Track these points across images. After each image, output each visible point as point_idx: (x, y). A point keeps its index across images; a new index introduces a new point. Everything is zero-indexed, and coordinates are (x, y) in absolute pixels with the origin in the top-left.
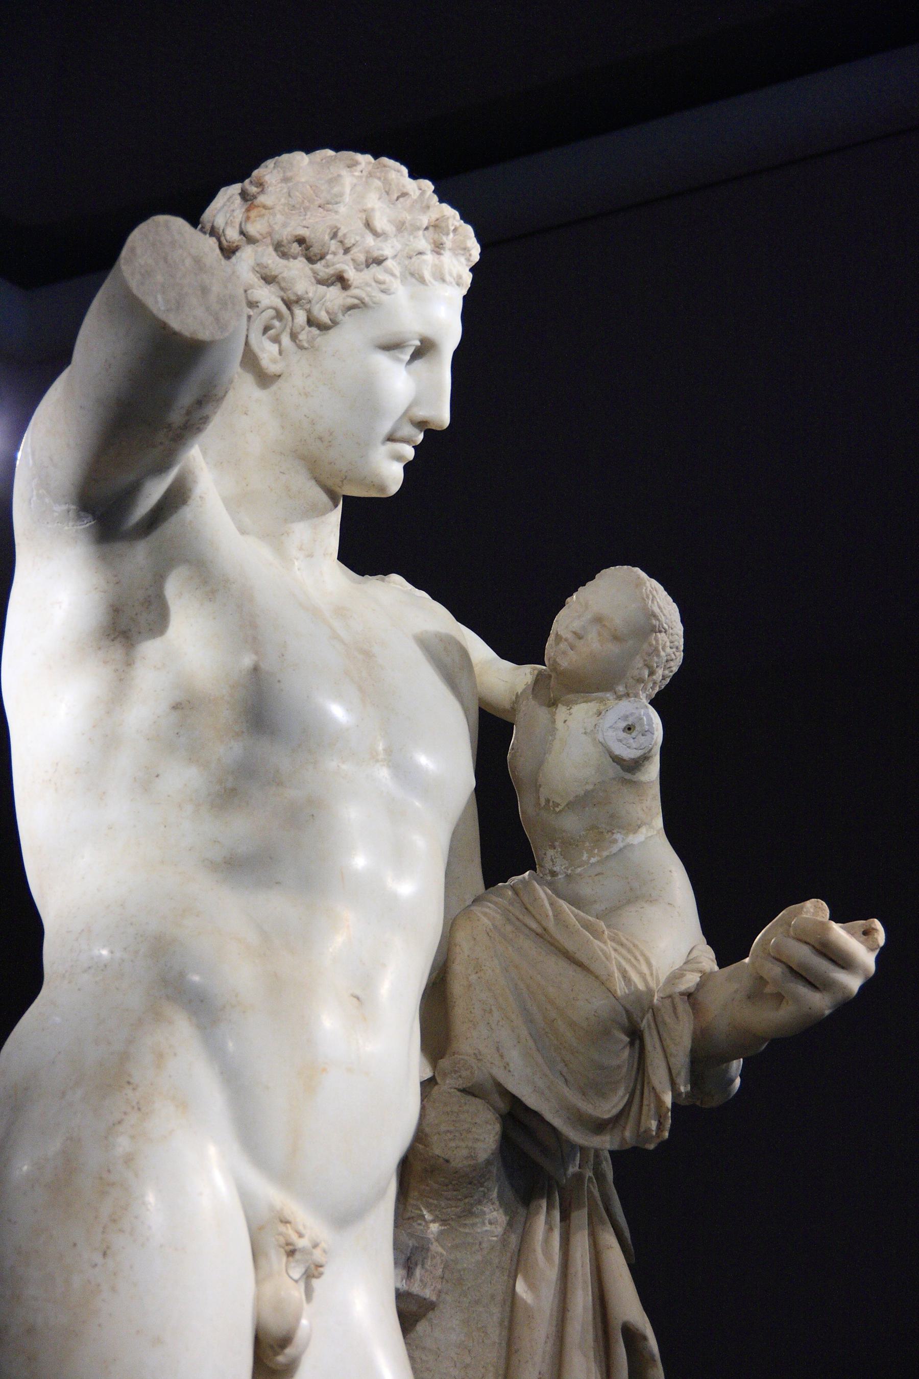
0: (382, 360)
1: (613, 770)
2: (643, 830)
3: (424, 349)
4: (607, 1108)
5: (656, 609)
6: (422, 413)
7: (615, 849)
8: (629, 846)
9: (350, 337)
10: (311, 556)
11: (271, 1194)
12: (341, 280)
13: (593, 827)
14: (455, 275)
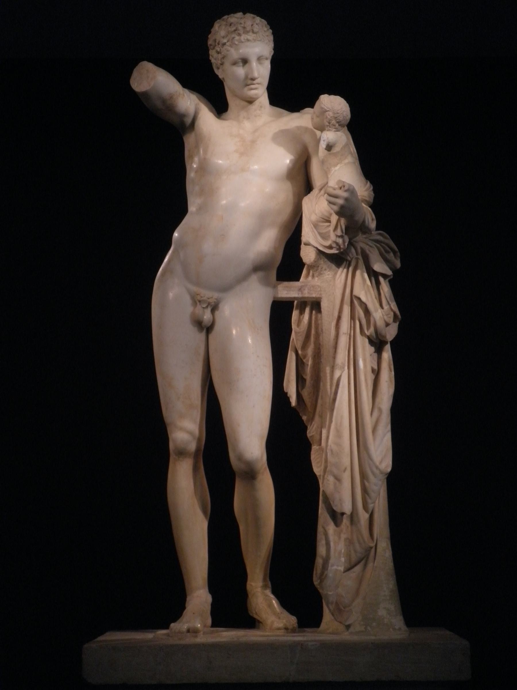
1: (326, 152)
2: (339, 165)
4: (327, 243)
5: (323, 106)
6: (249, 77)
7: (332, 172)
9: (227, 65)
11: (194, 289)
12: (218, 53)
14: (246, 38)
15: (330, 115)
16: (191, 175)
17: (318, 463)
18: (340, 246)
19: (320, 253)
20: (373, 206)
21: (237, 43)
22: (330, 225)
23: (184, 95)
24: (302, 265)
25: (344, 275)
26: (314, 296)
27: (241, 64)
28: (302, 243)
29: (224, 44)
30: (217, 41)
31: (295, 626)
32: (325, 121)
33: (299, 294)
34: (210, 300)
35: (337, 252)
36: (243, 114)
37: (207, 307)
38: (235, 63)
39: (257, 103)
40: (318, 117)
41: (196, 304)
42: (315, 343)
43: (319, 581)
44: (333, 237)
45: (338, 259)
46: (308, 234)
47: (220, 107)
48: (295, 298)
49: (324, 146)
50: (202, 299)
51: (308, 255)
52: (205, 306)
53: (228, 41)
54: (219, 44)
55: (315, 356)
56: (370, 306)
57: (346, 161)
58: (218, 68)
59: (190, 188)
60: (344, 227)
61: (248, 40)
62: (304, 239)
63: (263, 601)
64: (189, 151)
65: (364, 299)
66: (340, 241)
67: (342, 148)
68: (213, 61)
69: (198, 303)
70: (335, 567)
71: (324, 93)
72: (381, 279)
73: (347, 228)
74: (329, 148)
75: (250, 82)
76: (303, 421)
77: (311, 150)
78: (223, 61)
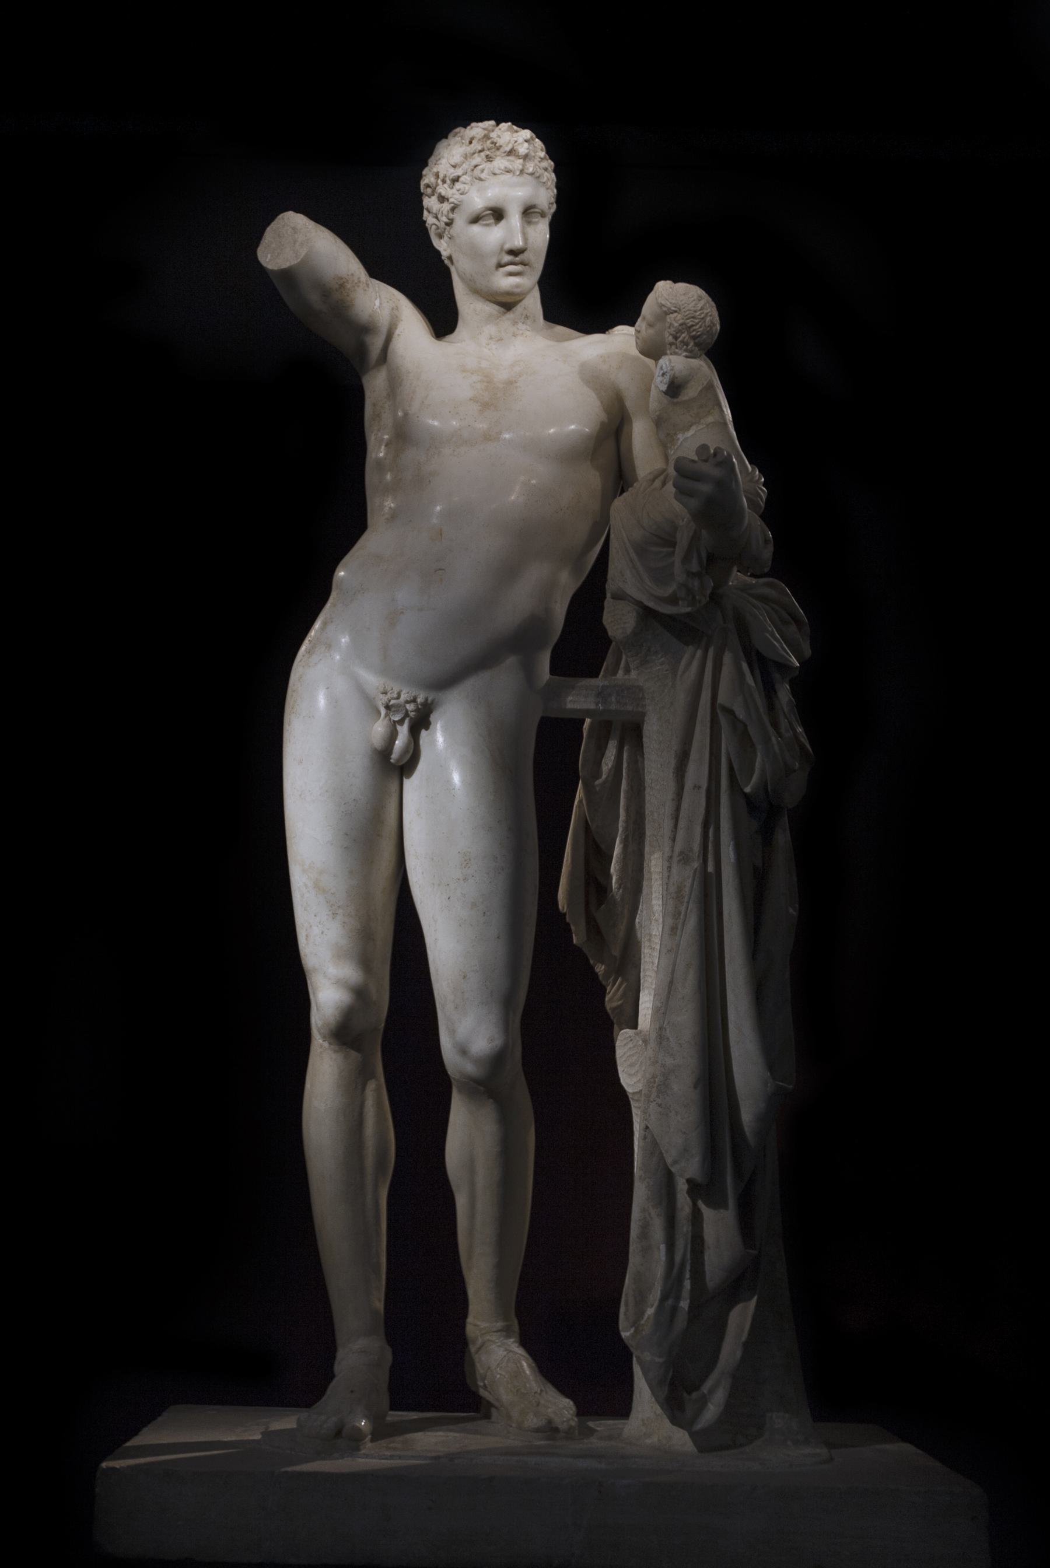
0: (476, 229)
1: (666, 400)
2: (694, 427)
3: (498, 214)
6: (507, 246)
8: (686, 439)
10: (501, 339)
13: (668, 434)
15: (675, 320)
16: (377, 451)
17: (631, 1065)
18: (694, 597)
19: (647, 614)
20: (768, 516)
21: (483, 176)
22: (673, 552)
23: (368, 285)
24: (610, 642)
25: (695, 664)
26: (629, 708)
27: (492, 221)
28: (608, 595)
29: (455, 180)
30: (441, 176)
31: (573, 1424)
32: (667, 335)
33: (597, 705)
34: (410, 707)
35: (689, 610)
36: (490, 329)
37: (401, 722)
38: (476, 220)
39: (519, 309)
40: (650, 325)
41: (379, 713)
42: (627, 810)
43: (632, 1330)
44: (679, 573)
45: (685, 630)
46: (622, 575)
47: (443, 320)
48: (588, 713)
49: (664, 388)
50: (392, 702)
51: (619, 620)
52: (397, 718)
53: (465, 173)
54: (444, 182)
55: (627, 837)
56: (753, 732)
57: (710, 419)
58: (441, 237)
59: (371, 477)
60: (704, 555)
61: (508, 171)
62: (611, 586)
63: (500, 1359)
64: (374, 405)
65: (741, 714)
66: (696, 583)
67: (701, 391)
68: (429, 220)
69: (383, 711)
70: (670, 1302)
71: (665, 278)
72: (777, 676)
73: (711, 558)
74: (674, 388)
75: (507, 258)
76: (596, 974)
77: (629, 404)
78: (451, 216)
